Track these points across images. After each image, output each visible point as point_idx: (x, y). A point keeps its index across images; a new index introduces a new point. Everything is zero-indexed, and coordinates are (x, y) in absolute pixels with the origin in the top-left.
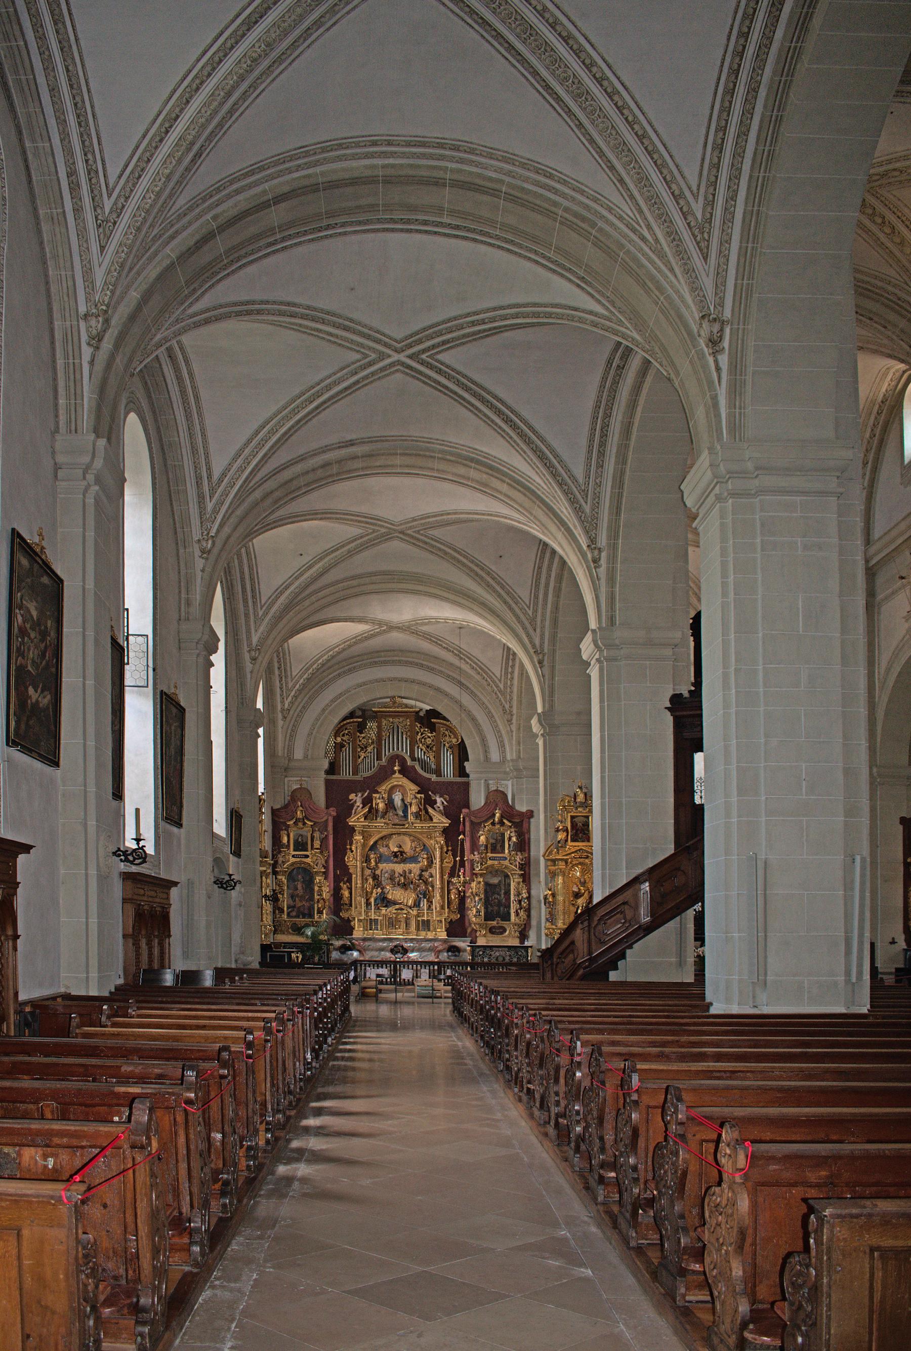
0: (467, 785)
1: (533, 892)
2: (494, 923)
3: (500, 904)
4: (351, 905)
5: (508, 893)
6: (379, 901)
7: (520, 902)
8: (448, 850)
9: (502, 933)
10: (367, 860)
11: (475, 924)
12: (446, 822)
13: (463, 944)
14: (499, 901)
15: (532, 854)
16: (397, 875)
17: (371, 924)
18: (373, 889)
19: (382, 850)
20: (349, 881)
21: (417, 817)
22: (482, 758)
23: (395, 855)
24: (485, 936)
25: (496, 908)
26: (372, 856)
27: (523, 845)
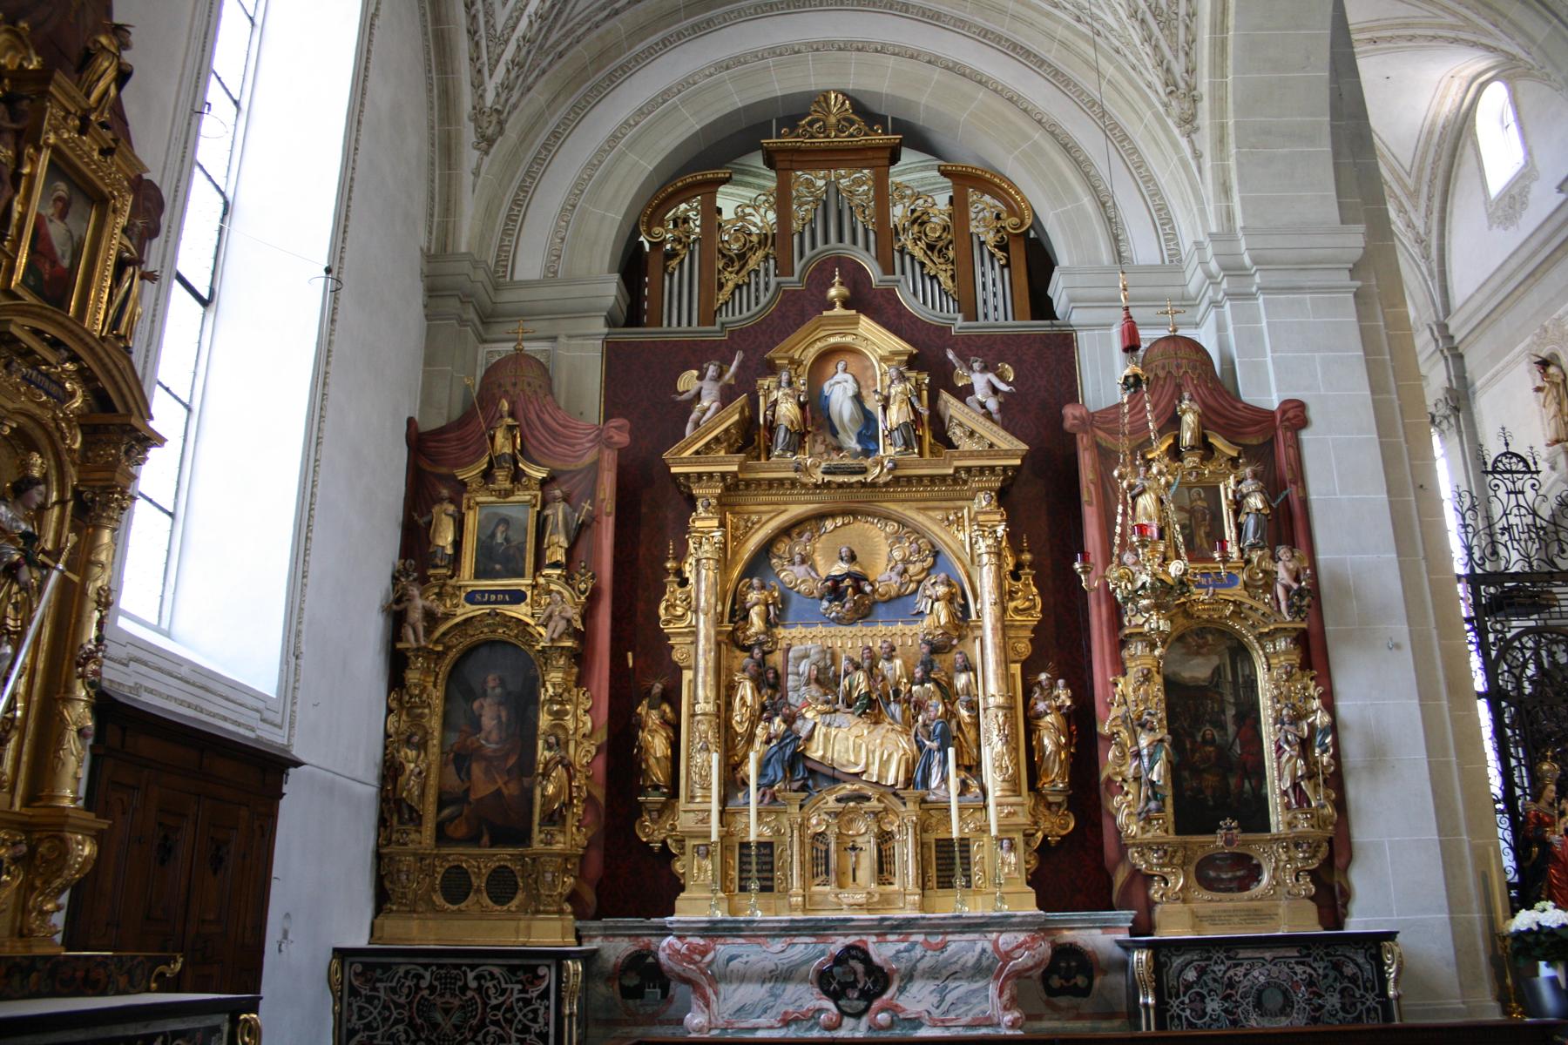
0: (1063, 346)
1: (1346, 706)
2: (1217, 841)
3: (1223, 762)
4: (674, 794)
5: (1249, 715)
6: (776, 771)
7: (1305, 746)
8: (1019, 565)
9: (1243, 886)
10: (739, 613)
11: (1145, 848)
12: (1010, 448)
13: (1100, 935)
14: (1223, 751)
15: (1321, 557)
16: (844, 664)
17: (756, 867)
18: (753, 725)
19: (791, 574)
20: (672, 696)
21: (907, 444)
22: (1105, 256)
23: (834, 590)
24: (1183, 897)
25: (1210, 780)
26: (753, 596)
27: (1287, 523)
